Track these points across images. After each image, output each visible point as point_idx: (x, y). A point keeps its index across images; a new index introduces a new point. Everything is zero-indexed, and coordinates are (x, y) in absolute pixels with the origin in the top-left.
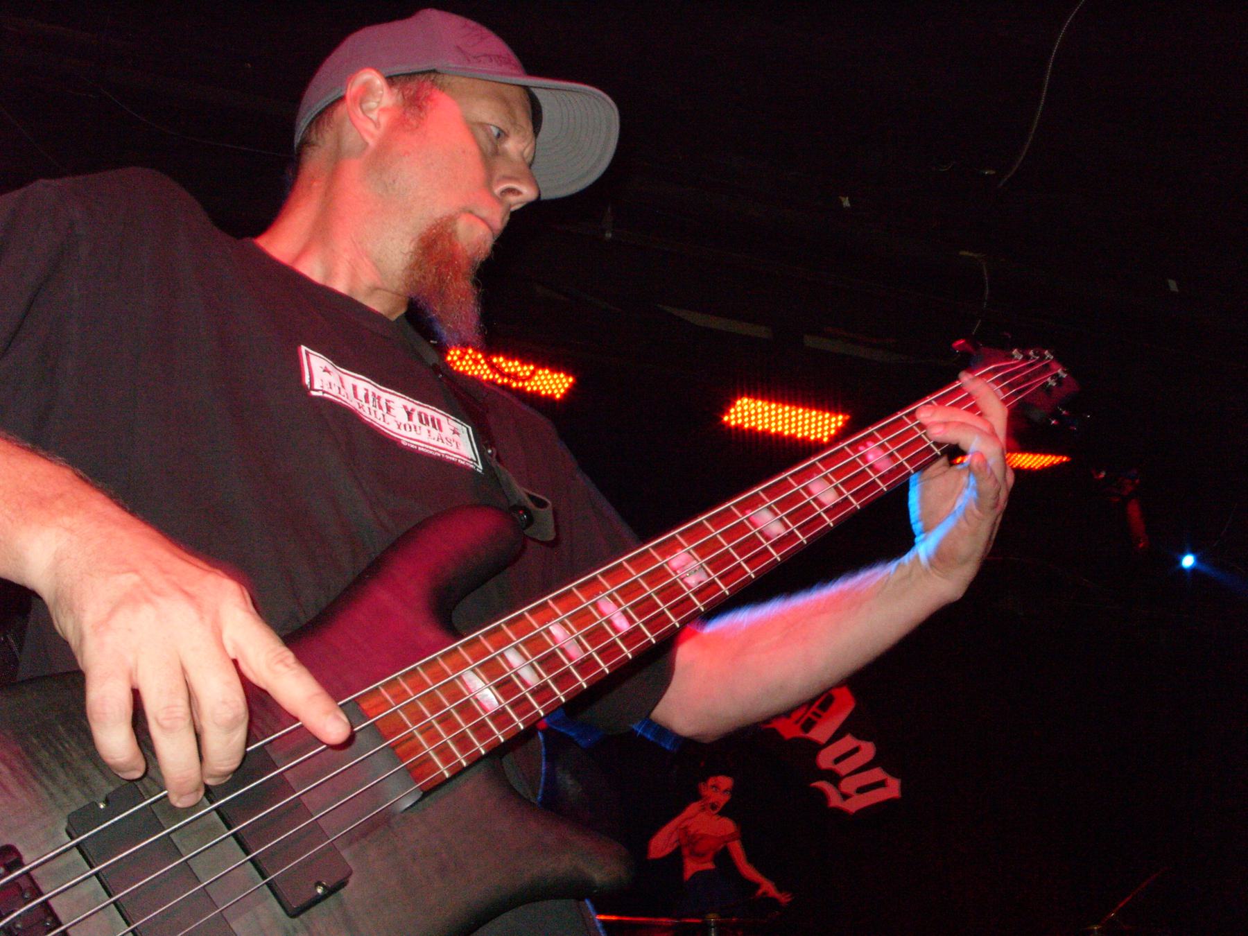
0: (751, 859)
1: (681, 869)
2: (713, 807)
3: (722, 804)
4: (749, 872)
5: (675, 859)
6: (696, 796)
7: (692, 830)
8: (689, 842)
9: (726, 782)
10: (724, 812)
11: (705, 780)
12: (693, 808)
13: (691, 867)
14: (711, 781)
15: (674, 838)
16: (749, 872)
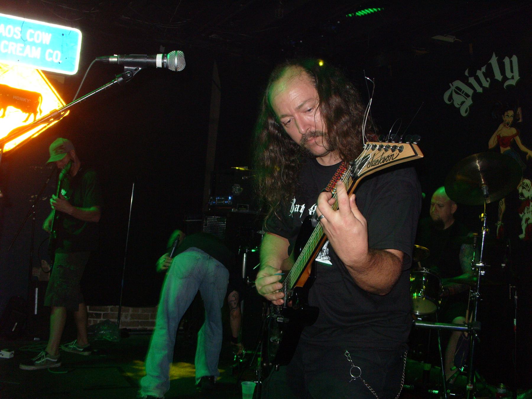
0: (523, 144)
1: (500, 151)
2: (508, 124)
3: (510, 122)
4: (523, 148)
5: (497, 149)
6: (502, 121)
7: (501, 136)
8: (502, 141)
9: (511, 113)
10: (512, 126)
11: (504, 114)
12: (501, 126)
13: (503, 150)
14: (506, 114)
15: (496, 139)
16: (523, 148)
